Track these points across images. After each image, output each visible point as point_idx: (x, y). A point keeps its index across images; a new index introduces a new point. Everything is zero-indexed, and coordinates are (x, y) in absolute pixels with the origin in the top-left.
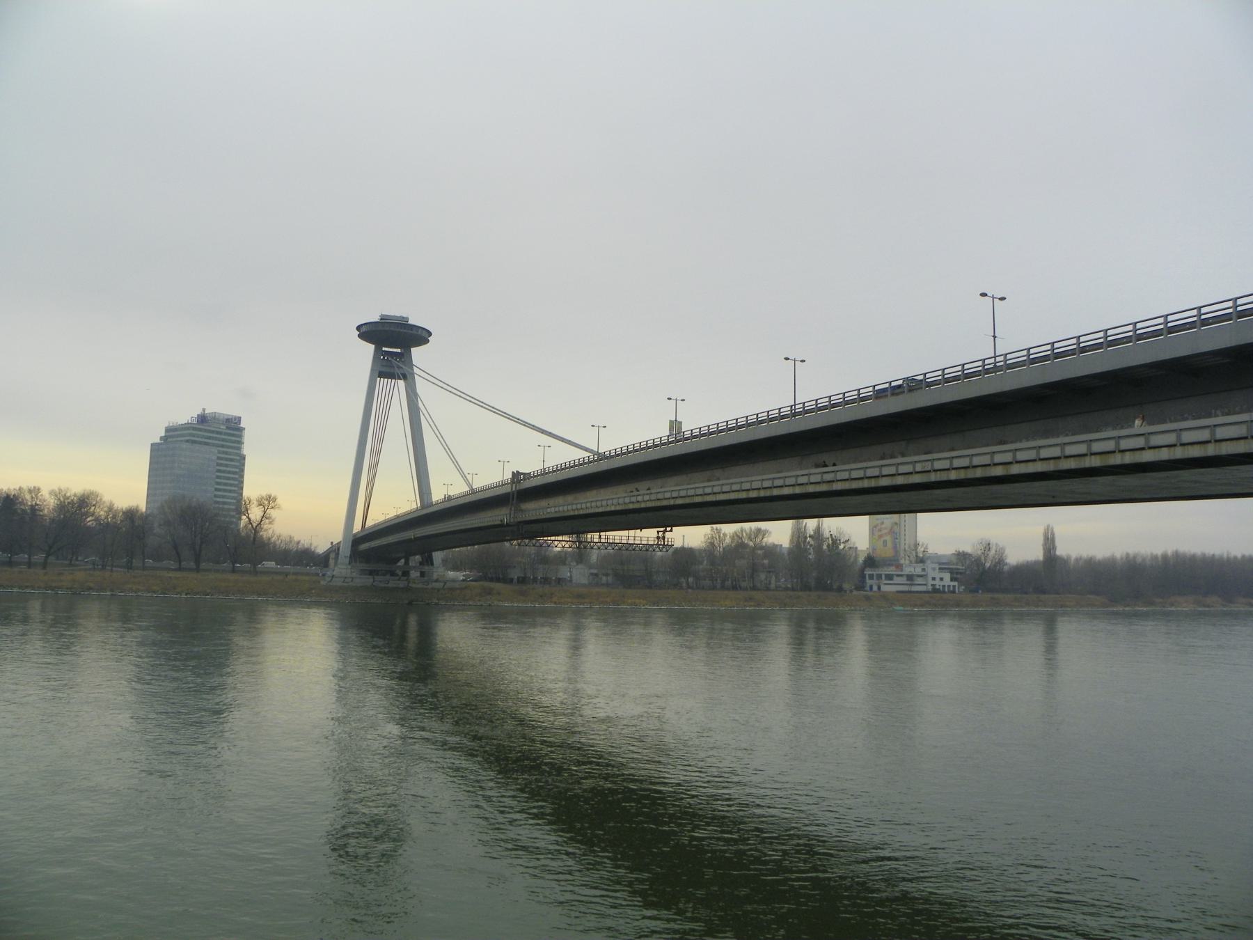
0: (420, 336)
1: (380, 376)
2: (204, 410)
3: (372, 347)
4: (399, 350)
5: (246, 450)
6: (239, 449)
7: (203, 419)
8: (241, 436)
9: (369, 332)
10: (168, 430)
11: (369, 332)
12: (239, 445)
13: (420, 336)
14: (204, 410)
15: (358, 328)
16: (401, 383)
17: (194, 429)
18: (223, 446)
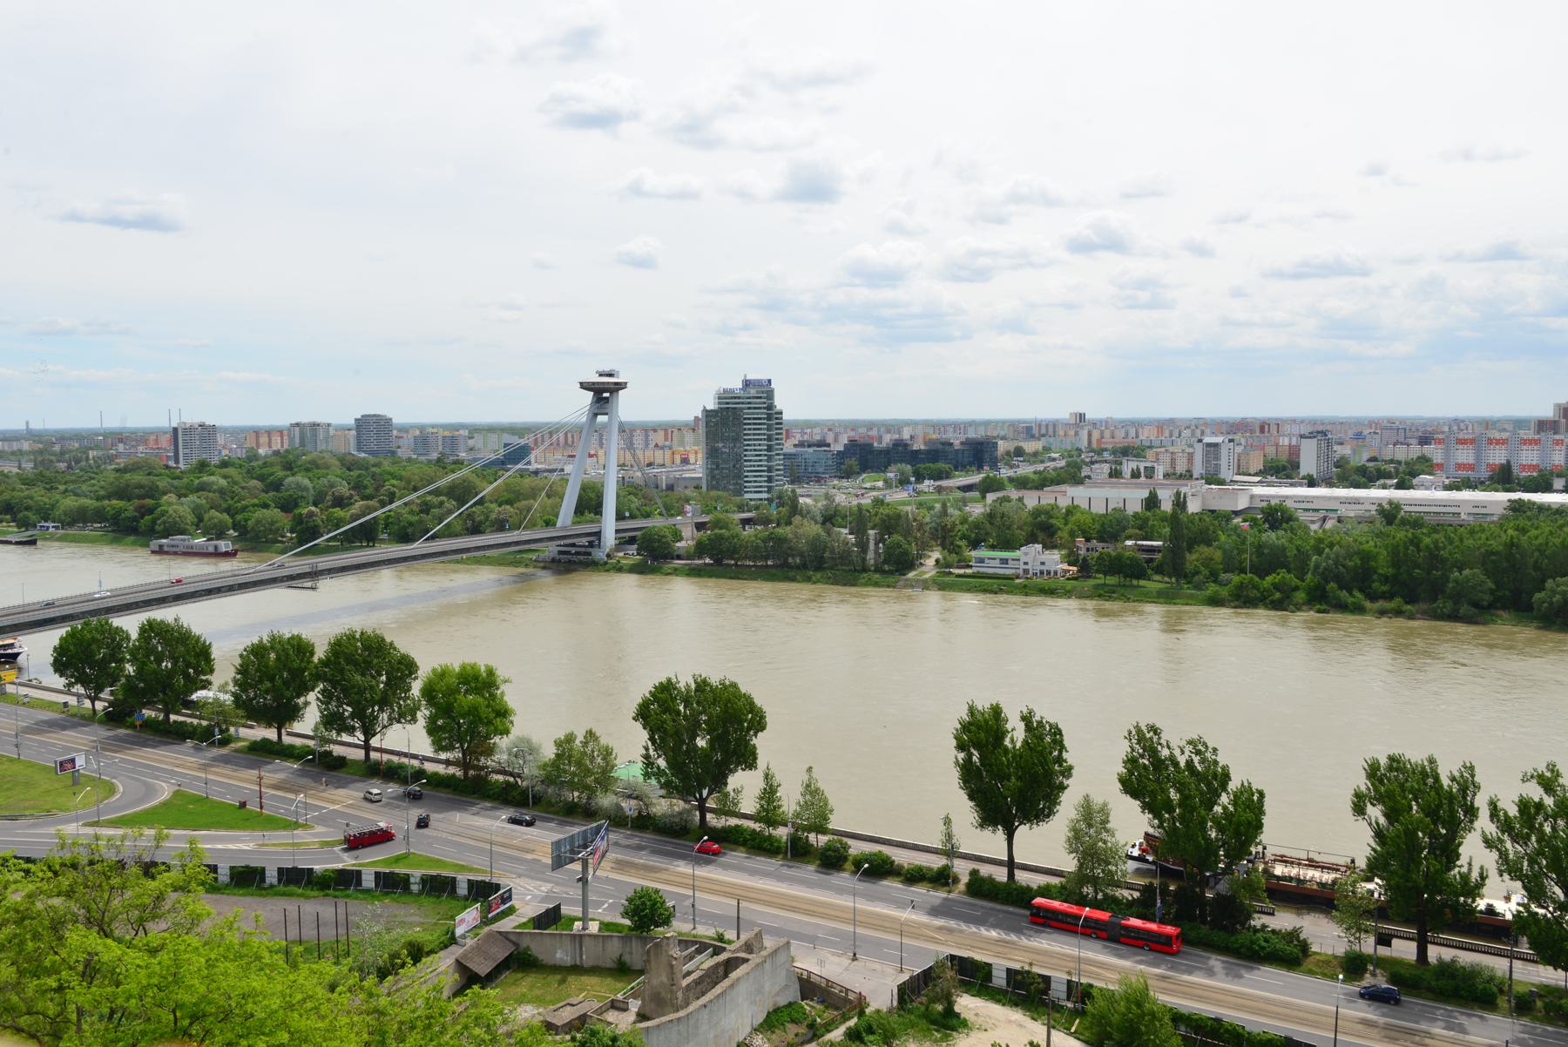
9: (584, 386)
11: (584, 386)
15: (581, 383)
18: (749, 408)
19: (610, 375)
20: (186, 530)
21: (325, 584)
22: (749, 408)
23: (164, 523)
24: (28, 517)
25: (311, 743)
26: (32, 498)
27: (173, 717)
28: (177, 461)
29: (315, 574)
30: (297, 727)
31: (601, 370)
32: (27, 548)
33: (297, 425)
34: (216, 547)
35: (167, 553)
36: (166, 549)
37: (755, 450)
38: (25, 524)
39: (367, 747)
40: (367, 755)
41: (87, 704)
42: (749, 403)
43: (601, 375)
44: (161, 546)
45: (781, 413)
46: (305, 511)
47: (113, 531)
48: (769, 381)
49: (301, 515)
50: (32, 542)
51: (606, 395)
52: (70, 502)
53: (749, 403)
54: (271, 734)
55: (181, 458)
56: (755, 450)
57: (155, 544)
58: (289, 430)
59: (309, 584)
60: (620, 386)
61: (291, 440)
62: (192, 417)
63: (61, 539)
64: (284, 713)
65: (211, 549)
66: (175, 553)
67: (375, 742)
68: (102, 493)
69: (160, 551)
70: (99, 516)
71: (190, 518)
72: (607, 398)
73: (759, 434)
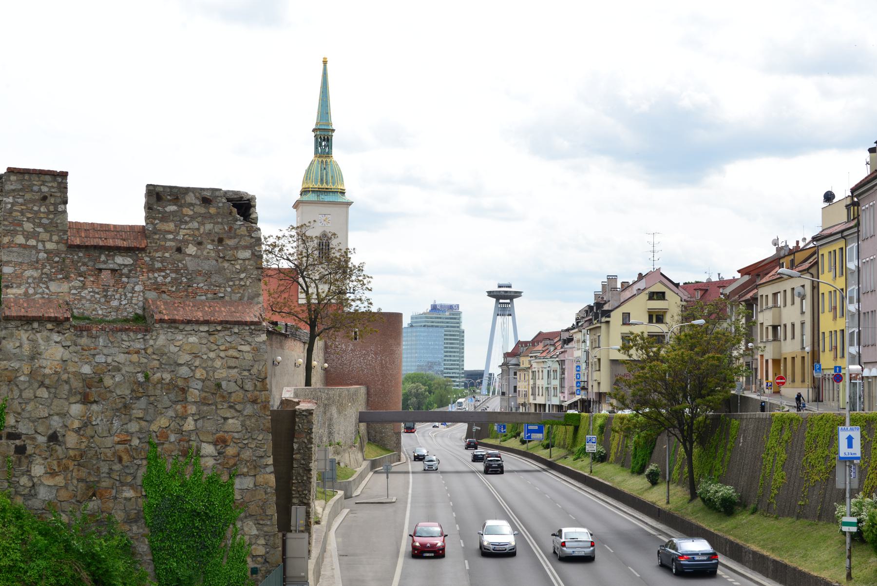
0: (518, 294)
1: (498, 315)
2: (435, 301)
3: (495, 299)
4: (508, 301)
5: (463, 326)
6: (458, 327)
7: (434, 308)
8: (459, 319)
9: (491, 294)
10: (412, 318)
11: (491, 294)
12: (458, 325)
13: (513, 296)
14: (435, 301)
16: (510, 317)
17: (427, 318)
18: (447, 327)
19: (510, 287)
22: (447, 327)
31: (502, 282)
37: (451, 360)
42: (447, 323)
43: (500, 287)
45: (463, 332)
48: (458, 306)
51: (501, 301)
53: (447, 323)
56: (451, 360)
60: (518, 294)
72: (509, 303)
73: (452, 348)
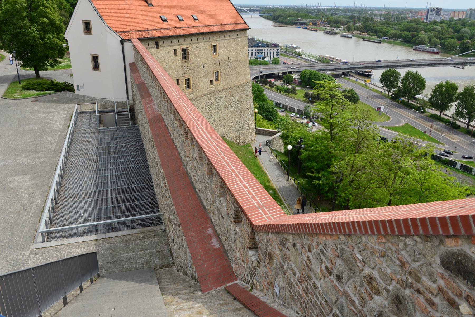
20: (425, 43)
21: (467, 67)
23: (419, 40)
24: (380, 35)
25: (450, 119)
26: (382, 29)
27: (410, 102)
28: (426, 20)
29: (464, 64)
30: (447, 112)
32: (379, 44)
33: (470, 9)
34: (433, 50)
35: (418, 50)
36: (417, 49)
38: (379, 37)
39: (468, 125)
40: (468, 127)
41: (387, 93)
44: (416, 48)
46: (466, 41)
47: (403, 41)
49: (464, 42)
50: (380, 43)
52: (392, 31)
54: (438, 113)
55: (428, 20)
57: (414, 47)
58: (466, 11)
59: (461, 67)
61: (467, 15)
62: (435, 5)
63: (388, 42)
64: (443, 107)
65: (431, 51)
66: (420, 51)
67: (471, 123)
68: (402, 29)
69: (416, 50)
70: (400, 36)
71: (427, 40)
